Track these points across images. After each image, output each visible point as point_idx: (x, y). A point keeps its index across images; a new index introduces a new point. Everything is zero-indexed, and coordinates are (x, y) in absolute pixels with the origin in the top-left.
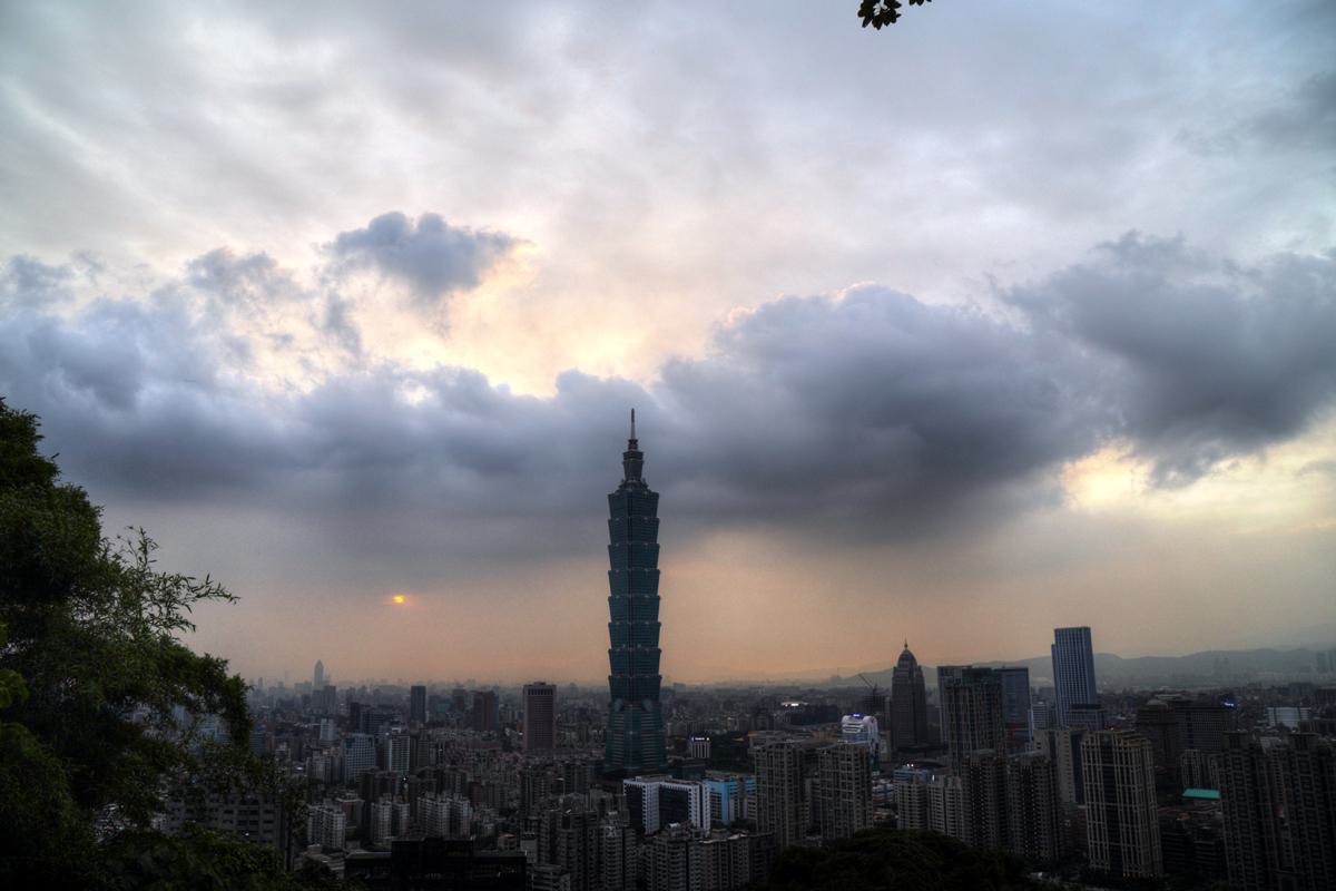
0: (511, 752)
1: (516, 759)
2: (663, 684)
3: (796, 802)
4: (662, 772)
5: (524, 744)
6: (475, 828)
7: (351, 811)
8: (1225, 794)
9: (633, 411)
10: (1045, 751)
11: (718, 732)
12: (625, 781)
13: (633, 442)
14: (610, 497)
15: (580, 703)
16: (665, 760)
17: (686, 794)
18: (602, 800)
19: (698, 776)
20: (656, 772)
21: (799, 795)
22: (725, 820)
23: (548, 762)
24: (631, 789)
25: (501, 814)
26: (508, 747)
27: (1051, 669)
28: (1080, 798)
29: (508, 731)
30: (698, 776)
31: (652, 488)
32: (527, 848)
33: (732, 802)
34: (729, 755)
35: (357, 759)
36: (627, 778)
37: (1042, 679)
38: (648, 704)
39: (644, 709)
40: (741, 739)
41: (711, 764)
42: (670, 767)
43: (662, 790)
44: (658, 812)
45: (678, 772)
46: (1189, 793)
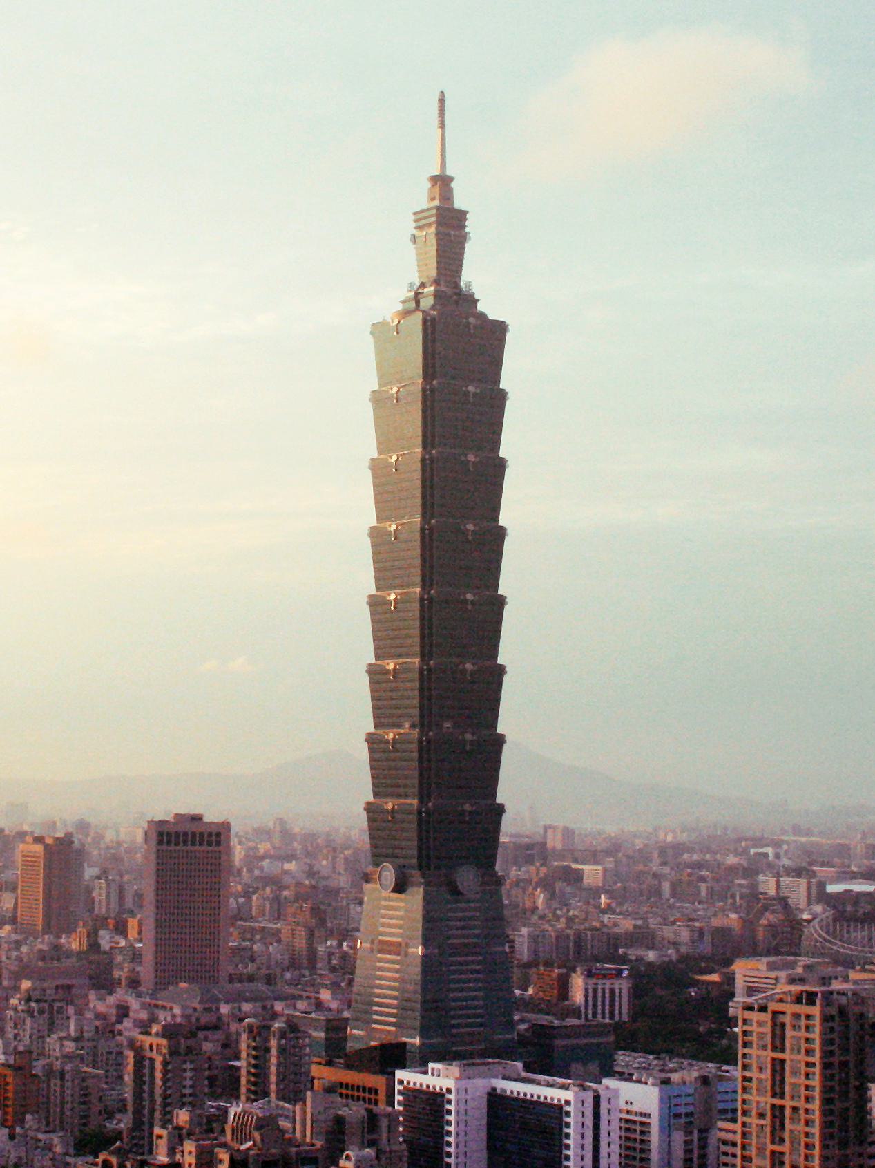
1: (123, 1011)
2: (509, 828)
3: (844, 1144)
4: (502, 1052)
5: (146, 971)
9: (442, 101)
11: (651, 956)
12: (400, 1074)
13: (442, 183)
14: (378, 330)
16: (511, 1025)
17: (557, 1112)
18: (340, 1121)
19: (594, 1067)
20: (483, 1054)
23: (205, 1019)
24: (413, 1095)
26: (104, 983)
29: (105, 939)
30: (594, 1067)
31: (490, 307)
33: (678, 1138)
34: (677, 1015)
36: (403, 1067)
38: (467, 878)
39: (456, 892)
40: (715, 977)
41: (628, 1039)
42: (523, 1041)
43: (496, 1101)
44: (484, 1154)
45: (543, 1056)
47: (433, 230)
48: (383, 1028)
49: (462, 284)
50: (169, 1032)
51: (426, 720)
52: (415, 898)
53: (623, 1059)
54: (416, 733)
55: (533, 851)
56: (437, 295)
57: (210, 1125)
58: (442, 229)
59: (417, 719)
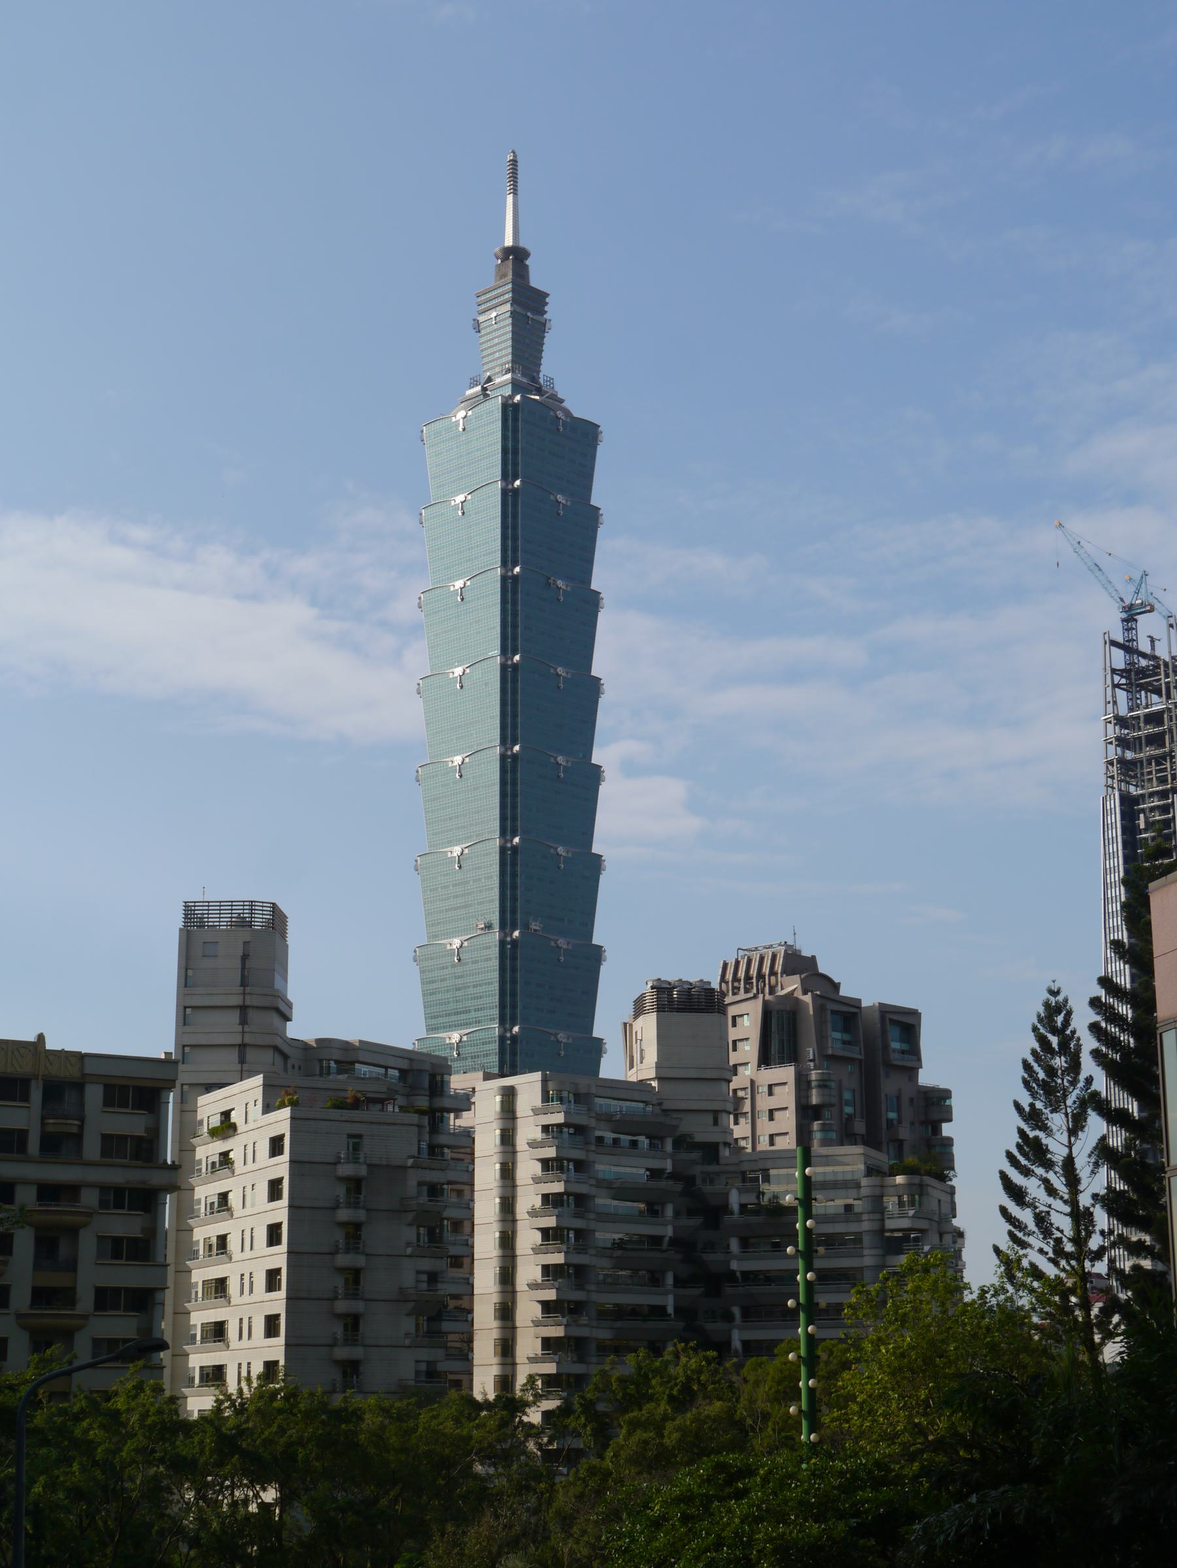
9: (514, 162)
31: (579, 405)
47: (508, 307)
49: (541, 381)
54: (496, 935)
56: (516, 386)
58: (519, 309)
59: (495, 918)
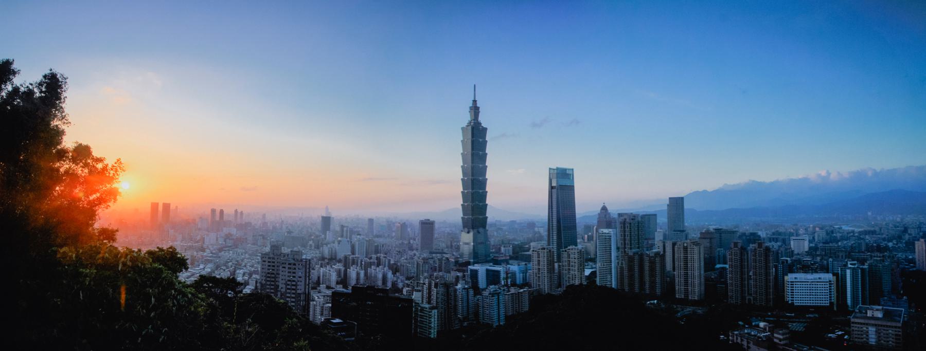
0: (412, 250)
2: (489, 221)
4: (487, 262)
6: (394, 284)
7: (339, 272)
8: (731, 266)
10: (661, 250)
15: (448, 230)
21: (551, 270)
22: (518, 282)
25: (408, 278)
26: (411, 249)
27: (666, 215)
28: (674, 269)
29: (412, 241)
32: (416, 296)
35: (343, 251)
37: (662, 220)
41: (511, 258)
45: (496, 262)
46: (718, 266)
48: (466, 258)
50: (424, 259)
51: (473, 201)
52: (471, 234)
53: (511, 262)
55: (492, 225)
57: (431, 276)
